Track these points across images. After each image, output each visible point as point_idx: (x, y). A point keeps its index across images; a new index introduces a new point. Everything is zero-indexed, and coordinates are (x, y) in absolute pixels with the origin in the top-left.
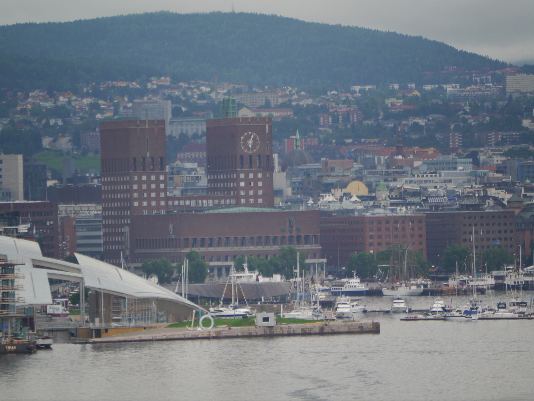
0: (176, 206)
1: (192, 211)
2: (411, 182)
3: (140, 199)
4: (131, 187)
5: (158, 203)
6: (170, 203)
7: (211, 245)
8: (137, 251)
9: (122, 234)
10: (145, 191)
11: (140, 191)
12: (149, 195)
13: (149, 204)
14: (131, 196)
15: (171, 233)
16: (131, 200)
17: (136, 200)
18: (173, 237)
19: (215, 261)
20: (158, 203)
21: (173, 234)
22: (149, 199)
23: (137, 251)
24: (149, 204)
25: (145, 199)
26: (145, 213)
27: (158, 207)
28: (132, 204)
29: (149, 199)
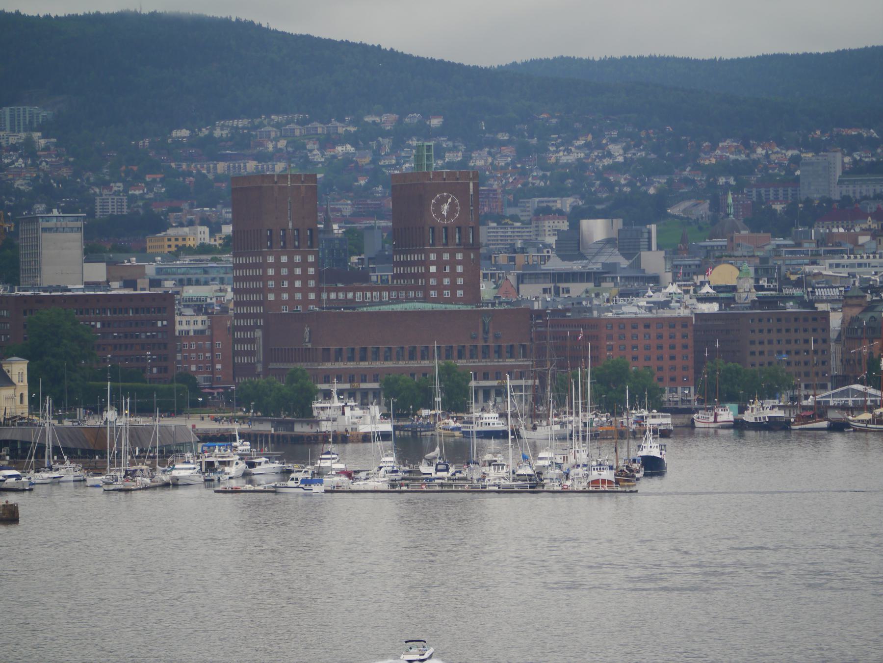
0: (333, 300)
1: (340, 309)
2: (838, 265)
3: (278, 291)
4: (265, 272)
5: (305, 296)
6: (324, 296)
7: (363, 359)
8: (273, 366)
9: (252, 341)
10: (285, 278)
11: (278, 278)
12: (291, 284)
13: (291, 297)
14: (265, 285)
15: (307, 340)
16: (264, 291)
17: (271, 291)
18: (310, 346)
19: (370, 382)
20: (305, 296)
21: (309, 342)
22: (292, 290)
23: (273, 366)
24: (291, 297)
25: (285, 290)
26: (285, 310)
27: (305, 301)
28: (265, 297)
29: (292, 290)
